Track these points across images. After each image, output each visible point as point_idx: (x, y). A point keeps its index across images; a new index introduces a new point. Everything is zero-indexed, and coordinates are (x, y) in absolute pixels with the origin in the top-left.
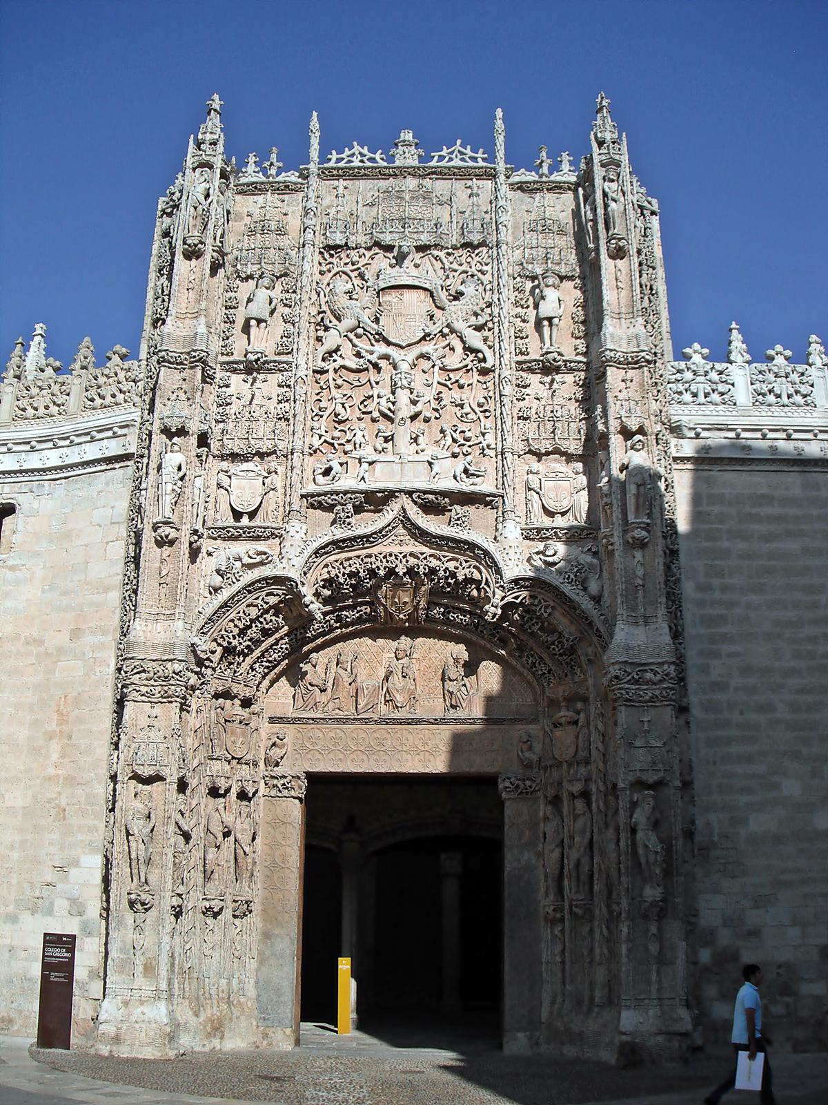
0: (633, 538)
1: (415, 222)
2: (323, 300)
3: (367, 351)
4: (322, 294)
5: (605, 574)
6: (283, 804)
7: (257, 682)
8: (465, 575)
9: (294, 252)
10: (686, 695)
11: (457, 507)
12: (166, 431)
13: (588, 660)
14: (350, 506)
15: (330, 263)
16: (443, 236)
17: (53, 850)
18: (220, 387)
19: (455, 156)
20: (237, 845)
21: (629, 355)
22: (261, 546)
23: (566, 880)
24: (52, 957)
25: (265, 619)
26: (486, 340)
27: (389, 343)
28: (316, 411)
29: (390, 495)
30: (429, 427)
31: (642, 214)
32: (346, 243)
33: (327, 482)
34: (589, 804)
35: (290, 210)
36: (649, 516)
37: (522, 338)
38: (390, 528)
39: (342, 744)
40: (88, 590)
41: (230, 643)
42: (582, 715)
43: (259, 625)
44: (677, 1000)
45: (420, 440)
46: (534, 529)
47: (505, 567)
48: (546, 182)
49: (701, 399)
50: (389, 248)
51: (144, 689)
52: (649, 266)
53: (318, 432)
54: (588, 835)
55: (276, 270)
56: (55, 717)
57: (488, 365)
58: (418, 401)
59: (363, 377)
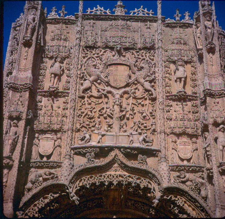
2: (83, 68)
3: (102, 90)
8: (144, 185)
12: (11, 118)
14: (93, 153)
16: (135, 44)
19: (140, 11)
21: (216, 92)
22: (52, 171)
26: (153, 86)
27: (112, 87)
29: (111, 149)
32: (94, 46)
38: (111, 164)
41: (34, 215)
46: (175, 166)
47: (163, 182)
48: (178, 23)
57: (153, 97)
59: (100, 101)
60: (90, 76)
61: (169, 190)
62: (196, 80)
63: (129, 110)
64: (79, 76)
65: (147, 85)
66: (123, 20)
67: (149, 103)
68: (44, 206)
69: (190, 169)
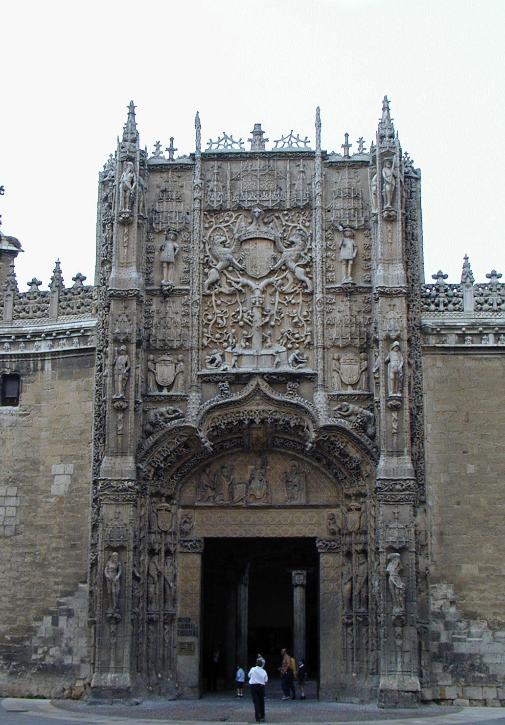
0: (391, 405)
2: (207, 248)
4: (207, 244)
12: (116, 341)
14: (226, 384)
15: (212, 222)
18: (146, 306)
20: (166, 583)
26: (307, 274)
28: (205, 322)
29: (250, 376)
30: (274, 331)
32: (221, 208)
33: (212, 367)
34: (366, 557)
36: (402, 392)
37: (331, 271)
41: (159, 465)
42: (363, 505)
45: (269, 340)
49: (442, 308)
51: (112, 497)
52: (412, 220)
53: (207, 335)
54: (365, 575)
55: (177, 228)
60: (218, 260)
61: (326, 428)
62: (369, 260)
63: (275, 312)
65: (300, 272)
67: (303, 301)
68: (169, 454)
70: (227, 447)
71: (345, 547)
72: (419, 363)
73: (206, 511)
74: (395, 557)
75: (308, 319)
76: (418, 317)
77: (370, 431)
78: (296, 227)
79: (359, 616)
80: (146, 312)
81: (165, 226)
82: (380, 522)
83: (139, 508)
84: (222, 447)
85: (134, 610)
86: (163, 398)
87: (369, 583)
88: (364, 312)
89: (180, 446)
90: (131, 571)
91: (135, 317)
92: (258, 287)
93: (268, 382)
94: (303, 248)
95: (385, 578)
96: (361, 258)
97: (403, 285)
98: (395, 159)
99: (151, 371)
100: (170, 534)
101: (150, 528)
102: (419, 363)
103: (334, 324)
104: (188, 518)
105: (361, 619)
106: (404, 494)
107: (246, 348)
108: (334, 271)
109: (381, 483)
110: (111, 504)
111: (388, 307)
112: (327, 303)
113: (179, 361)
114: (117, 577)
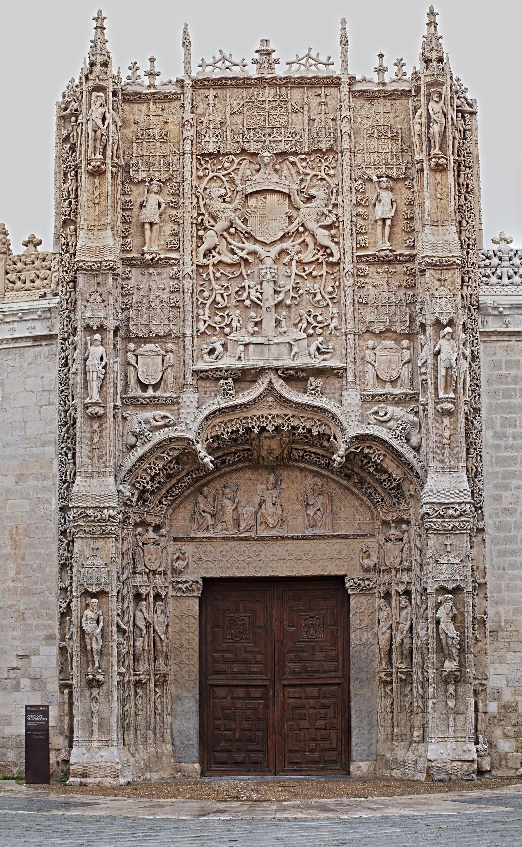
0: (442, 408)
1: (275, 131)
3: (239, 248)
4: (201, 198)
5: (423, 429)
6: (187, 602)
7: (164, 512)
9: (176, 158)
10: (482, 520)
11: (312, 379)
13: (411, 495)
14: (230, 380)
15: (207, 169)
17: (15, 643)
18: (123, 279)
20: (156, 635)
21: (444, 259)
23: (394, 654)
24: (33, 721)
25: (169, 467)
26: (333, 236)
27: (256, 241)
28: (201, 300)
29: (261, 371)
30: (290, 312)
31: (463, 117)
32: (219, 151)
33: (212, 360)
34: (410, 600)
35: (170, 117)
36: (455, 391)
39: (229, 555)
40: (28, 443)
42: (406, 534)
43: (165, 472)
44: (467, 738)
45: (283, 324)
49: (505, 280)
50: (255, 154)
53: (203, 318)
54: (408, 623)
56: (9, 542)
57: (334, 260)
58: (280, 292)
61: (359, 438)
64: (195, 222)
66: (274, 85)
67: (327, 272)
68: (158, 472)
69: (396, 399)
70: (231, 462)
71: (382, 587)
72: (476, 353)
73: (205, 543)
74: (446, 599)
75: (334, 296)
76: (475, 292)
77: (414, 440)
78: (317, 176)
79: (401, 673)
80: (122, 288)
81: (145, 174)
82: (428, 556)
83: (121, 542)
84: (224, 462)
85: (120, 671)
86: (148, 400)
87: (414, 631)
88: (406, 287)
89: (170, 462)
90: (115, 623)
91: (111, 297)
92: (268, 254)
93: (284, 379)
94: (326, 202)
95: (434, 626)
96: (401, 217)
97: (457, 255)
98: (445, 90)
99: (131, 365)
100: (160, 574)
101: (134, 568)
102: (476, 353)
103: (367, 303)
104: (181, 553)
105: (404, 677)
106: (458, 521)
107: (253, 334)
108: (366, 233)
109: (430, 508)
110: (87, 538)
111: (438, 283)
112: (358, 275)
113: (167, 352)
114: (99, 630)
